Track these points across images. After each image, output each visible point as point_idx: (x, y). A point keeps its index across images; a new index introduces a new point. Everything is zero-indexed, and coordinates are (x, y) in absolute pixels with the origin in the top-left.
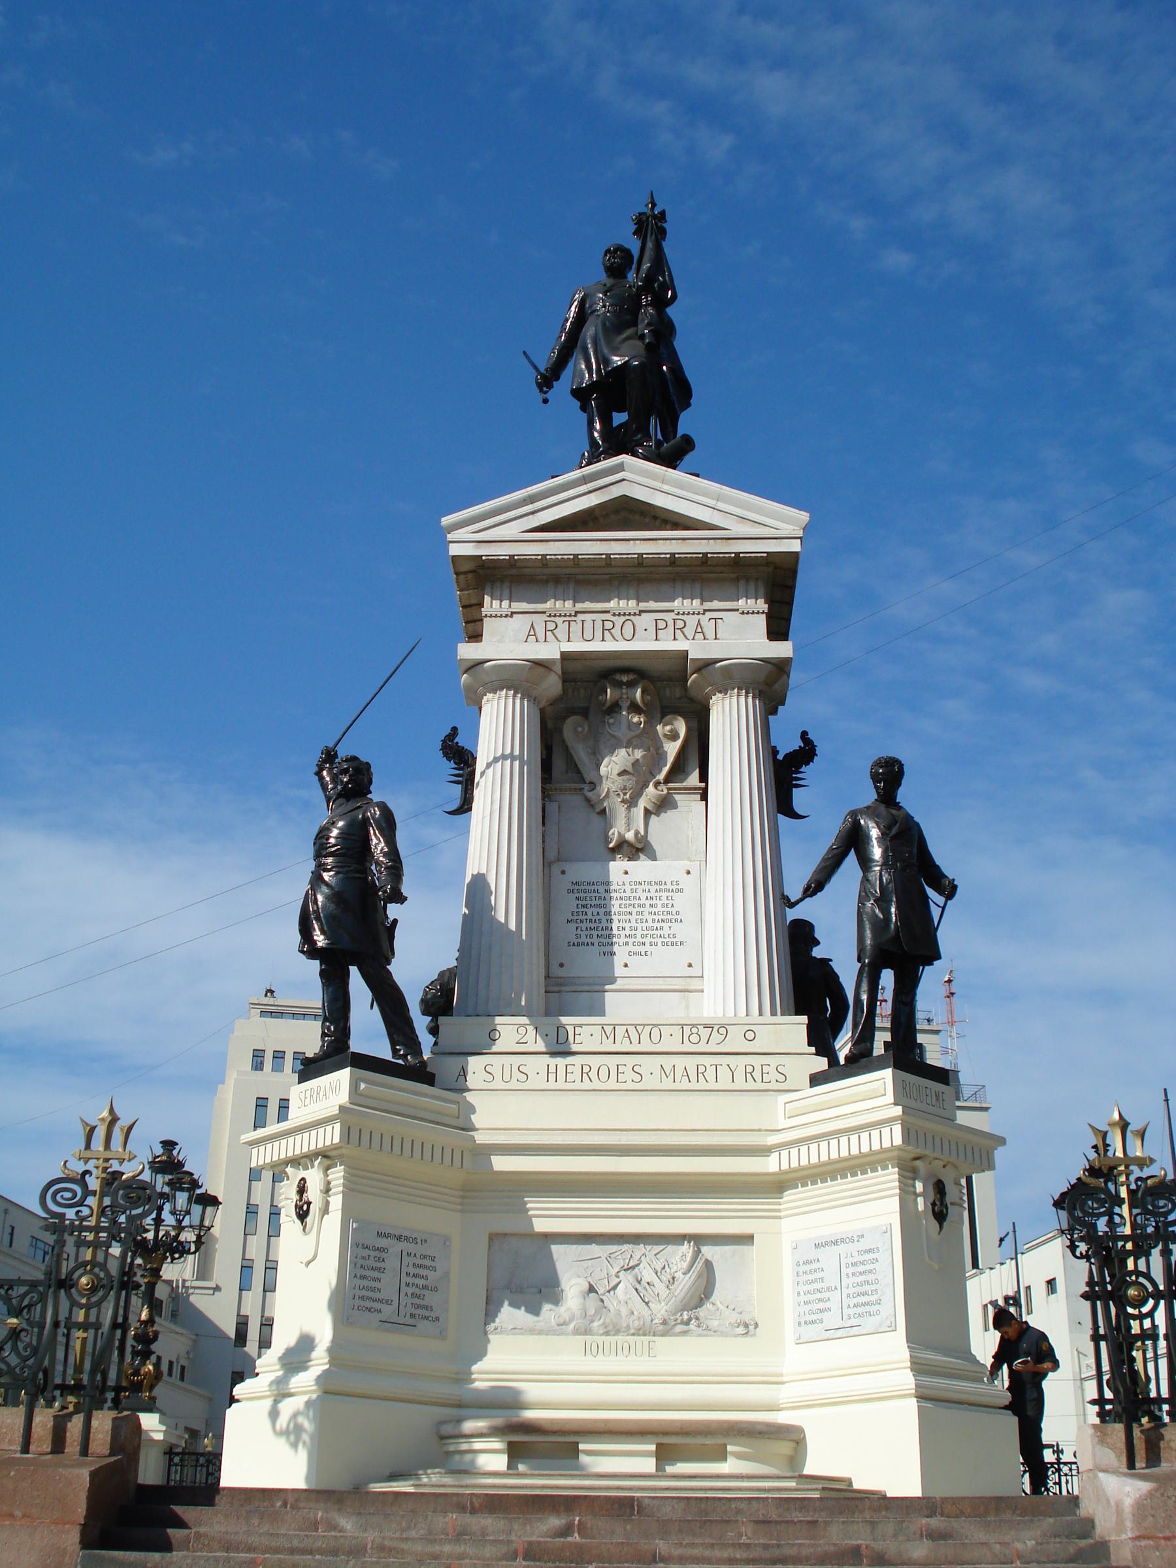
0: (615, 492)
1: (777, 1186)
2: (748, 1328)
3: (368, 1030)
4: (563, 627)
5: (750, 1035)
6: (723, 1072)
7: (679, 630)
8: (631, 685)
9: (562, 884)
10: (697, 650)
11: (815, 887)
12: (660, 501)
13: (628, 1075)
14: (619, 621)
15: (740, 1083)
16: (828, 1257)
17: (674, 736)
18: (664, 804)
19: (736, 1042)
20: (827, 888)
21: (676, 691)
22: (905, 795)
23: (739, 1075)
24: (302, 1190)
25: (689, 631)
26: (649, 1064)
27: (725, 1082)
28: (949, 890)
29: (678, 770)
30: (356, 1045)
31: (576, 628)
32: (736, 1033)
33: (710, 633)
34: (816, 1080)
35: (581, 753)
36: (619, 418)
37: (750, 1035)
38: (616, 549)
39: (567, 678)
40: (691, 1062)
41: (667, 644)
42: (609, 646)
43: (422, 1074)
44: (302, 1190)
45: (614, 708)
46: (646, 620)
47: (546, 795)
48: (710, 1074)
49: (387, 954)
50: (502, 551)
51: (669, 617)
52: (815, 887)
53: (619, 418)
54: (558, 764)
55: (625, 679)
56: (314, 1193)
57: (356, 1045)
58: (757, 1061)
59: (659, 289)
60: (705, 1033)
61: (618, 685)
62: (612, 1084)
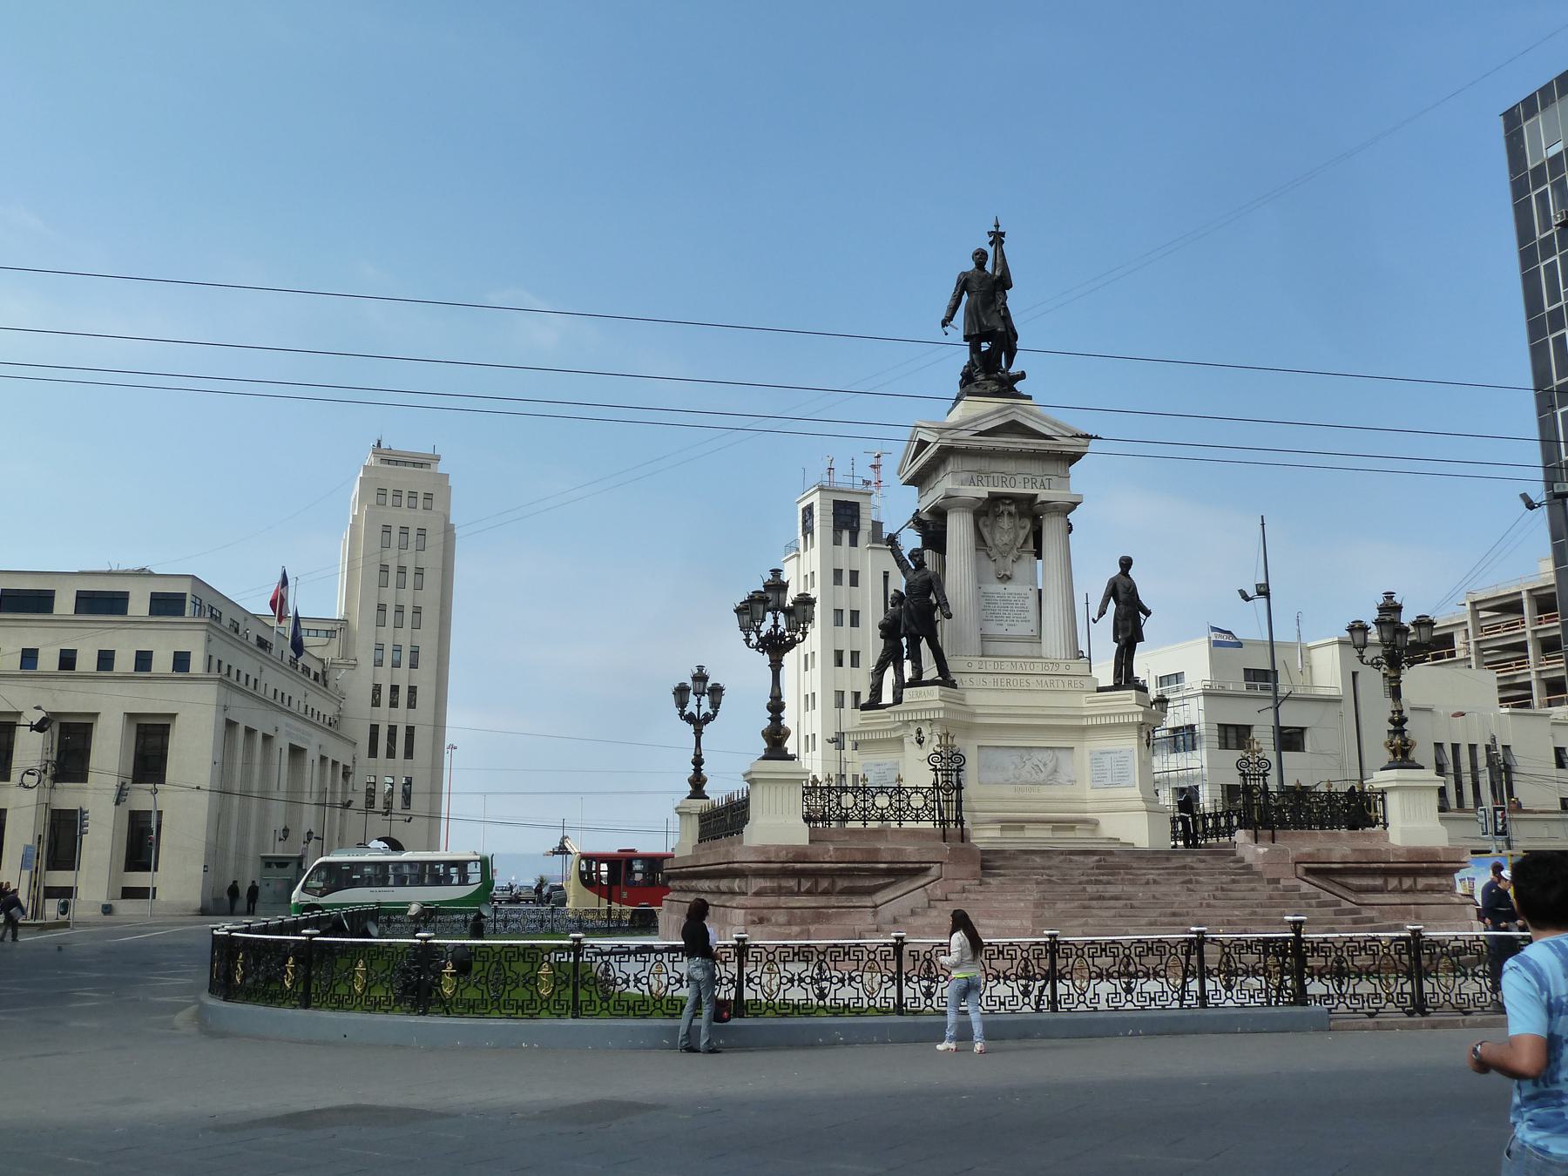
1: (1084, 729)
2: (1073, 782)
5: (1068, 667)
6: (1060, 683)
10: (1044, 495)
11: (1102, 613)
12: (1030, 424)
16: (1107, 759)
18: (1019, 558)
19: (1062, 671)
24: (919, 732)
26: (1032, 679)
28: (1148, 613)
29: (1026, 541)
32: (1062, 666)
34: (1100, 690)
36: (985, 346)
37: (1068, 667)
43: (953, 685)
44: (919, 732)
46: (1019, 478)
52: (1102, 613)
53: (985, 346)
56: (925, 733)
59: (1004, 282)
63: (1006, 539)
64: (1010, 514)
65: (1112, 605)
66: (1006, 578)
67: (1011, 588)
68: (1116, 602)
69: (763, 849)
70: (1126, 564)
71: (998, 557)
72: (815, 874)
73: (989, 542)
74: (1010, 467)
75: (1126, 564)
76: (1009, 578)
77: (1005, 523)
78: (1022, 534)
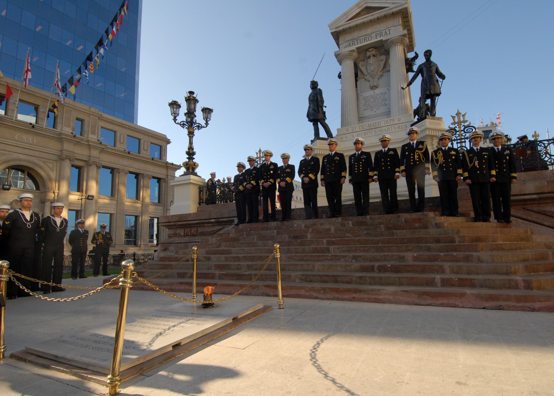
0: (364, 6)
3: (323, 133)
4: (356, 42)
7: (381, 35)
8: (372, 51)
9: (361, 98)
10: (384, 38)
13: (374, 132)
14: (368, 37)
15: (397, 130)
17: (382, 60)
18: (382, 76)
20: (413, 84)
21: (382, 49)
22: (432, 59)
23: (397, 128)
25: (383, 35)
27: (394, 130)
30: (321, 136)
31: (359, 41)
33: (388, 33)
35: (363, 69)
38: (365, 20)
39: (359, 53)
40: (386, 128)
41: (379, 39)
42: (366, 43)
45: (369, 57)
46: (374, 35)
47: (356, 81)
48: (390, 129)
49: (324, 118)
50: (341, 29)
51: (379, 33)
54: (359, 73)
55: (370, 50)
57: (321, 136)
58: (400, 125)
60: (389, 121)
61: (370, 51)
62: (370, 135)
63: (372, 68)
64: (374, 56)
65: (420, 78)
66: (373, 88)
67: (377, 91)
68: (422, 76)
69: (173, 216)
70: (428, 54)
71: (370, 79)
72: (190, 226)
73: (365, 73)
74: (369, 31)
75: (428, 54)
76: (376, 87)
77: (372, 60)
78: (382, 63)
